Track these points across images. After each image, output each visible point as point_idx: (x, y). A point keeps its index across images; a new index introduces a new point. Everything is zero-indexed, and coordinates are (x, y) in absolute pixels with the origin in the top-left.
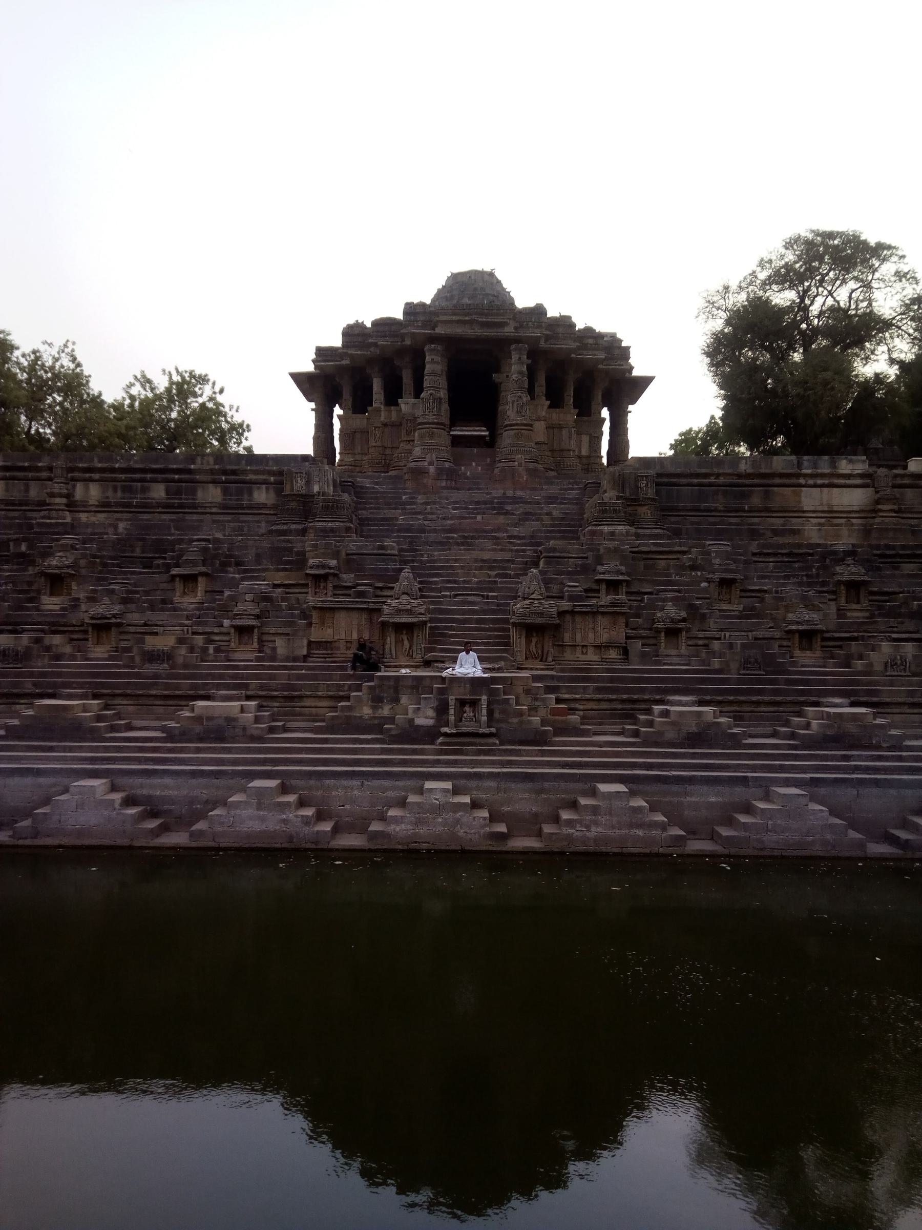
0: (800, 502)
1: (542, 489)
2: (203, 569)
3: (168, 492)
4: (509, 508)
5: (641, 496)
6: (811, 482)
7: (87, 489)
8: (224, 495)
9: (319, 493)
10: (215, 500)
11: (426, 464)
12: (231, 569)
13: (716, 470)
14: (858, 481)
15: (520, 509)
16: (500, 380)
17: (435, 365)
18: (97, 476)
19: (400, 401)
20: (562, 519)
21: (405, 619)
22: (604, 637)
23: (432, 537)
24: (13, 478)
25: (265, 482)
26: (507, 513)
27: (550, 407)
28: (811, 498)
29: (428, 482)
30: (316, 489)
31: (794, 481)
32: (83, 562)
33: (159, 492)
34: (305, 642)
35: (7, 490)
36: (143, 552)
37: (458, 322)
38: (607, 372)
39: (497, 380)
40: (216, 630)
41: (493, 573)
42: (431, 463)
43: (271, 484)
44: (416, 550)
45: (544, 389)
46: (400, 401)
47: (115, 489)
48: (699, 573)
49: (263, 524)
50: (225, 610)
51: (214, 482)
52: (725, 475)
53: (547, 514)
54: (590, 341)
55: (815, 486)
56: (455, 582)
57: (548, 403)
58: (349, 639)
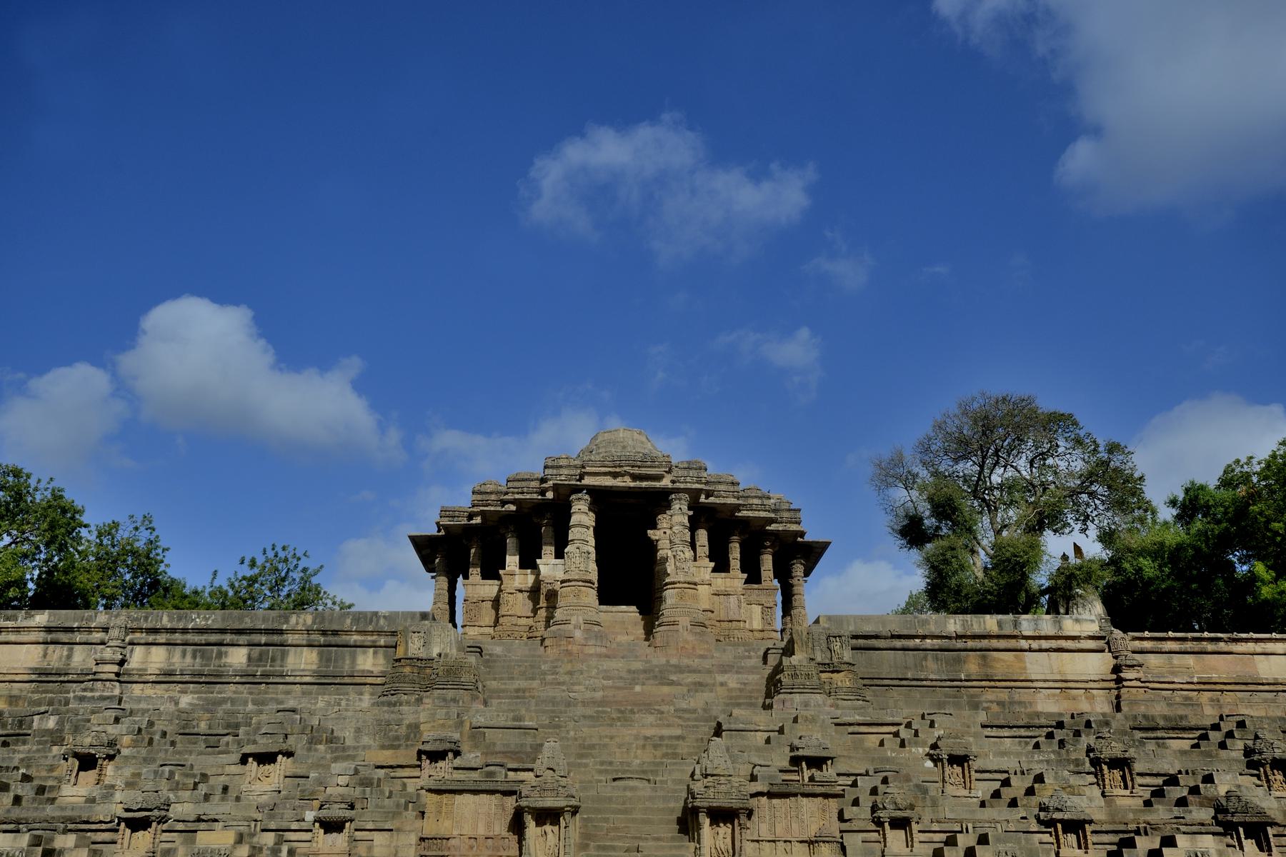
0: (1025, 668)
1: (713, 657)
2: (284, 747)
4: (674, 678)
5: (835, 660)
6: (1035, 645)
8: (321, 660)
9: (440, 655)
10: (309, 667)
11: (571, 627)
12: (321, 747)
13: (921, 632)
14: (1091, 644)
15: (690, 678)
17: (582, 518)
18: (162, 638)
19: (538, 561)
20: (741, 690)
21: (549, 803)
22: (811, 833)
23: (580, 710)
26: (672, 683)
27: (714, 570)
28: (1038, 665)
29: (575, 649)
30: (435, 652)
31: (1012, 643)
32: (126, 740)
33: (238, 657)
34: (413, 839)
35: (45, 655)
37: (605, 474)
38: (776, 534)
39: (653, 537)
40: (294, 826)
41: (659, 753)
42: (577, 627)
44: (558, 727)
45: (706, 549)
46: (538, 561)
47: (184, 654)
48: (921, 750)
49: (366, 697)
50: (307, 798)
53: (722, 684)
54: (756, 501)
55: (1040, 650)
56: (611, 763)
57: (712, 564)
58: (471, 834)
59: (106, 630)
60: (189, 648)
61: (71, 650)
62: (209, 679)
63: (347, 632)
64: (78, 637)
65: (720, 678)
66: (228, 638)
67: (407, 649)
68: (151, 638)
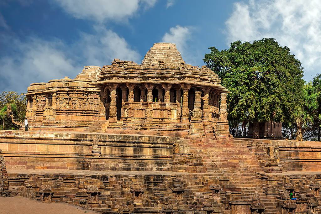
3: (135, 150)
7: (105, 149)
11: (199, 136)
16: (205, 100)
18: (107, 143)
24: (77, 144)
25: (167, 148)
35: (75, 149)
36: (154, 180)
43: (168, 148)
49: (168, 164)
51: (150, 147)
52: (293, 148)
59: (91, 141)
60: (117, 148)
61: (83, 147)
62: (123, 157)
63: (159, 144)
64: (84, 143)
65: (244, 156)
66: (127, 144)
67: (179, 151)
68: (105, 144)
